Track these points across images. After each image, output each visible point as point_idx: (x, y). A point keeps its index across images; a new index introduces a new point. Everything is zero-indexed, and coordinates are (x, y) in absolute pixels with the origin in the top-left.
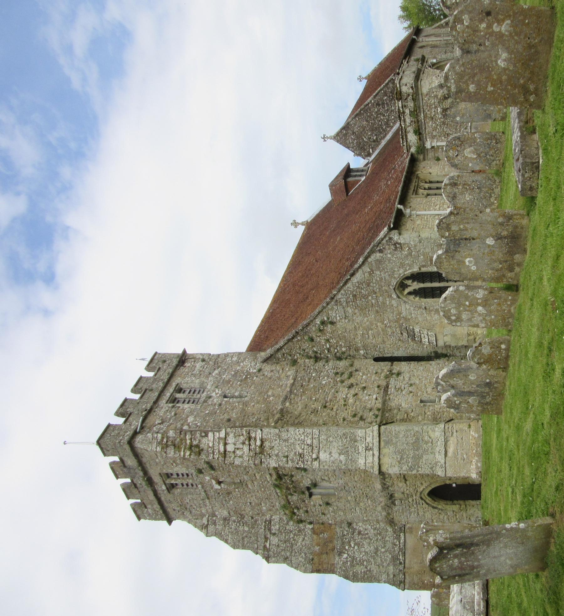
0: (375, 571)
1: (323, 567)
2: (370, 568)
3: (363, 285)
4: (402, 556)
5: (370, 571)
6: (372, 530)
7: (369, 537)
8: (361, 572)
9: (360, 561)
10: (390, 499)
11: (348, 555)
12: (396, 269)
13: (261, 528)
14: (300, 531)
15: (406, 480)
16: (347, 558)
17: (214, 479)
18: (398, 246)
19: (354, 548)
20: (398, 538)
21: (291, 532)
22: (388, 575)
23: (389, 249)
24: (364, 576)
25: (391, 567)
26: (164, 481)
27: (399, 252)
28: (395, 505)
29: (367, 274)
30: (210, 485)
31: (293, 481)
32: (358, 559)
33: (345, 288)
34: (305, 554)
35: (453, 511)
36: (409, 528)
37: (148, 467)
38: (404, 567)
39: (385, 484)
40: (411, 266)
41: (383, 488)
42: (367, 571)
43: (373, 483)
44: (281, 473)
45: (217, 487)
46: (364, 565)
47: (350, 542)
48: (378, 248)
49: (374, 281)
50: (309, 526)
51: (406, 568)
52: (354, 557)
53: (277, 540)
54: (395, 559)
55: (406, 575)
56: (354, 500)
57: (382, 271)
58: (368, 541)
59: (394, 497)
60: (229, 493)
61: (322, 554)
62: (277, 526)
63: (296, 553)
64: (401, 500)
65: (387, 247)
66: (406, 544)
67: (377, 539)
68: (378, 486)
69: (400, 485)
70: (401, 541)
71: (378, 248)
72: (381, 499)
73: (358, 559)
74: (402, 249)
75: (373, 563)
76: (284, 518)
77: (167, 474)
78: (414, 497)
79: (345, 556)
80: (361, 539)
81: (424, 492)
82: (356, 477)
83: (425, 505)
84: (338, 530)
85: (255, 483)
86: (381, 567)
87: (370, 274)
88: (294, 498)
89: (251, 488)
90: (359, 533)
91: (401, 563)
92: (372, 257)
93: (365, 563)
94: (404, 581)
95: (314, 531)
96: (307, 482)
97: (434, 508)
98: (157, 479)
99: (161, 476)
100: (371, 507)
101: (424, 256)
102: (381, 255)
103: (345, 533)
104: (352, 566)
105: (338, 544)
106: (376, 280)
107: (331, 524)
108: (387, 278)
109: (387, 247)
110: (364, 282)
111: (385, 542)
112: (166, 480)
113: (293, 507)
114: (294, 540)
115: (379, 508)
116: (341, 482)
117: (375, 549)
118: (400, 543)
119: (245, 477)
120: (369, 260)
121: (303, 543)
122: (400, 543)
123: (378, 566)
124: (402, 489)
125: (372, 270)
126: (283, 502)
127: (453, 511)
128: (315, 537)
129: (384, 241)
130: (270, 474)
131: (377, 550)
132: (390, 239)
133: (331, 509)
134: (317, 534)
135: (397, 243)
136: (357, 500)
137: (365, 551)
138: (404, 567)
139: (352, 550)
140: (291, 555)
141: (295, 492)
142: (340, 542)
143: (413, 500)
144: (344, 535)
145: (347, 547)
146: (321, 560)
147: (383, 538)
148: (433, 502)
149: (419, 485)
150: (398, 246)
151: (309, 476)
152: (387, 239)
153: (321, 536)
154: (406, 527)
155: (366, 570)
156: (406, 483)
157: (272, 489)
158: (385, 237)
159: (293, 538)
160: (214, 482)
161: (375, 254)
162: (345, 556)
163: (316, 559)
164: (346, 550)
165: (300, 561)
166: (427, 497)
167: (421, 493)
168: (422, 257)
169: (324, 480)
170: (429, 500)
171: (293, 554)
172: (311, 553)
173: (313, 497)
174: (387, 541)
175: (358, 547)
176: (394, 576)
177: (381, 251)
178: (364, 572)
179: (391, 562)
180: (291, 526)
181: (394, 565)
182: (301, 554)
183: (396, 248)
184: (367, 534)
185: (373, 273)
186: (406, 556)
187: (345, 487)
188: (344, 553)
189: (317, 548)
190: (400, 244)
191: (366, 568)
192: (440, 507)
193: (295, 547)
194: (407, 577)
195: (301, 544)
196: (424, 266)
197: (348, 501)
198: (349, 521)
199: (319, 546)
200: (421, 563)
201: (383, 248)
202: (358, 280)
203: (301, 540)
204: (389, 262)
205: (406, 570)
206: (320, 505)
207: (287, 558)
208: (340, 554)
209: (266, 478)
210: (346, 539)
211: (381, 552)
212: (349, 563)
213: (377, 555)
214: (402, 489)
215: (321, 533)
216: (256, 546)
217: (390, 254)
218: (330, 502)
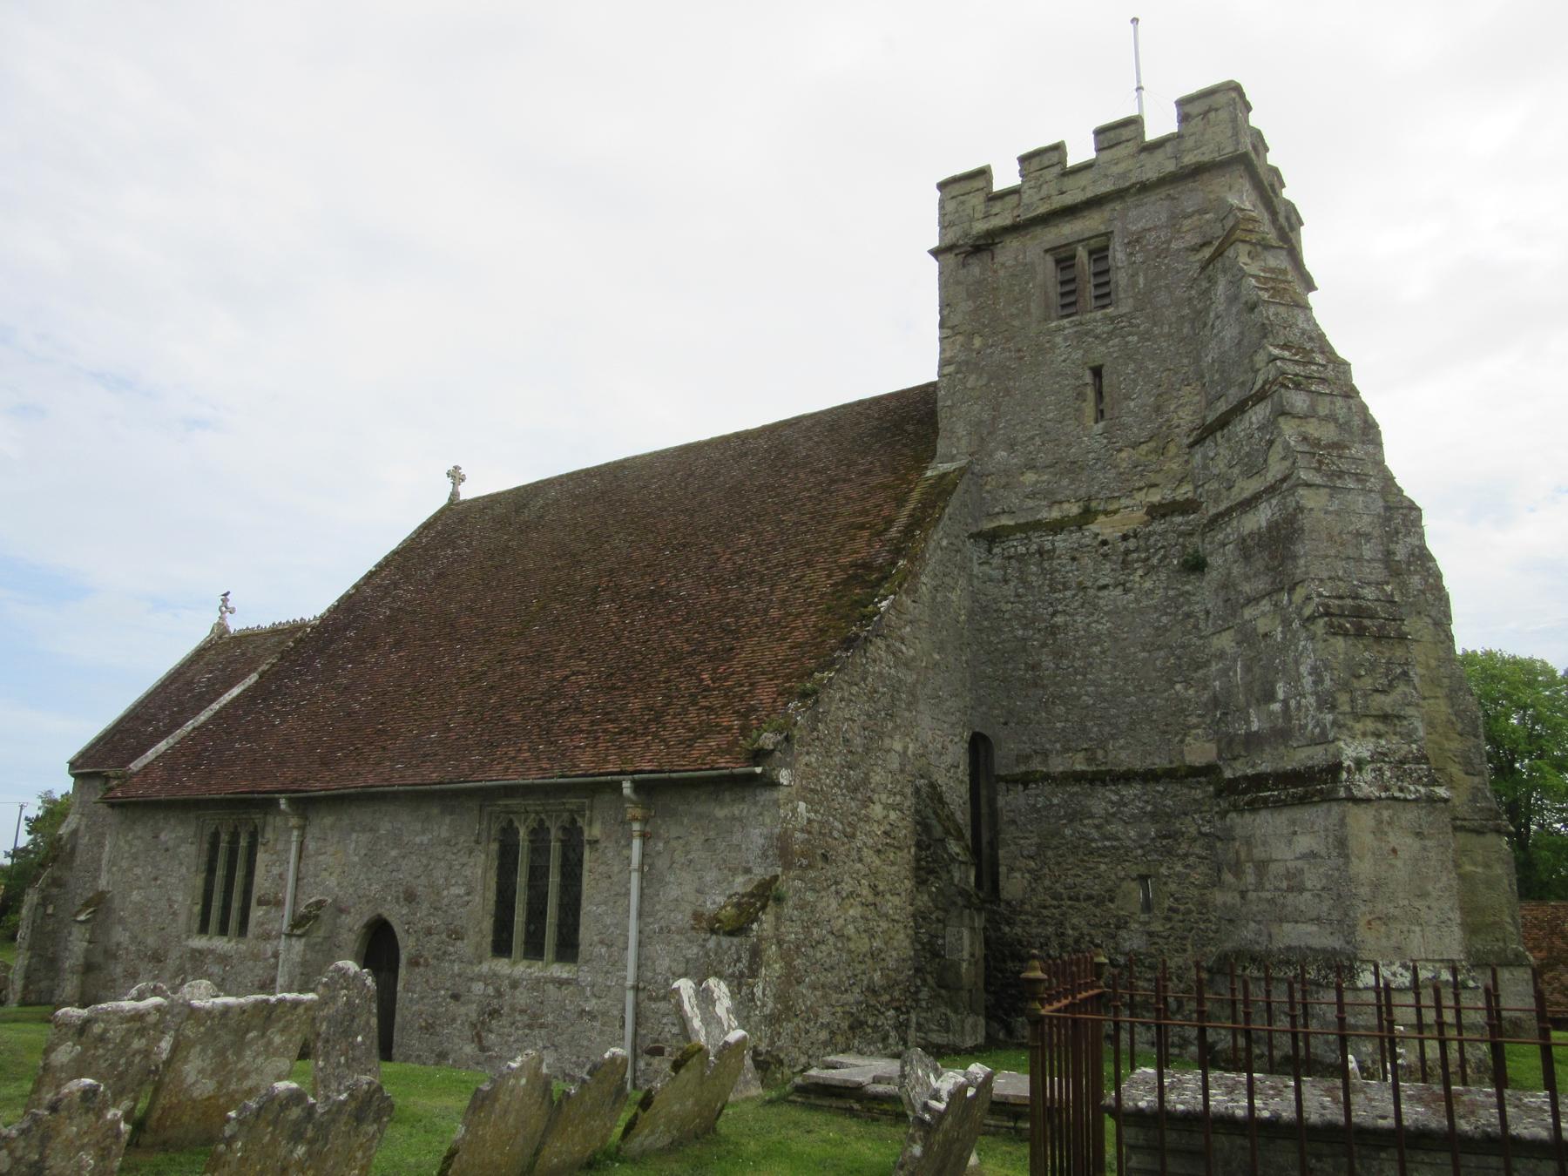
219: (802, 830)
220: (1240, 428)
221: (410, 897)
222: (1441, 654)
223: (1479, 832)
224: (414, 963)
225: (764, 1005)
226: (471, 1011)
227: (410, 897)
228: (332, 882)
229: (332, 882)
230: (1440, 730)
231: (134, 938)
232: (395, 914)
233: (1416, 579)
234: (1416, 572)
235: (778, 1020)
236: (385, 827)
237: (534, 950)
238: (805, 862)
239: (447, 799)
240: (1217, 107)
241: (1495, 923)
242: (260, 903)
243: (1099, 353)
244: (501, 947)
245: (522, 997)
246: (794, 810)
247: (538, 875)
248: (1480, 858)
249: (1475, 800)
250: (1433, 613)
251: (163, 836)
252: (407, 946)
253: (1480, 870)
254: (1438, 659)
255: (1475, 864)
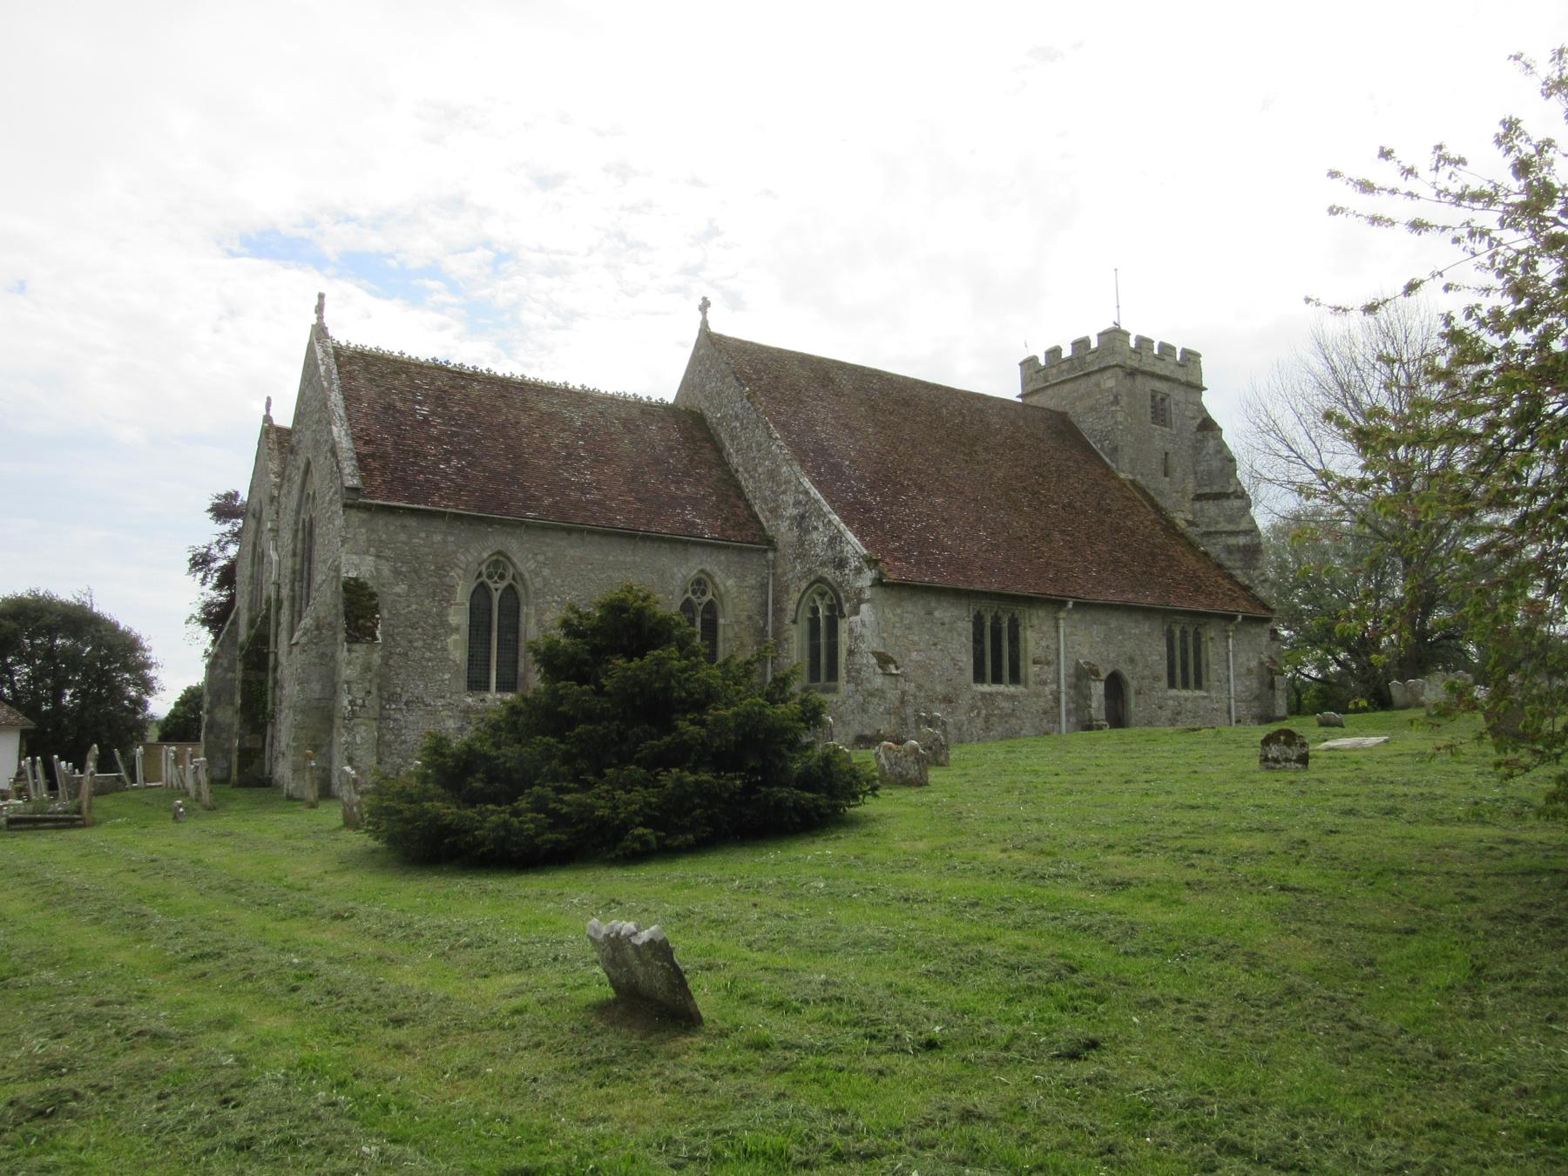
220: (1226, 503)
221: (1132, 660)
224: (1138, 693)
226: (1167, 713)
227: (1132, 660)
228: (1085, 651)
229: (1085, 651)
231: (919, 687)
232: (1126, 670)
236: (1114, 624)
237: (1186, 686)
239: (1148, 612)
240: (1191, 358)
242: (1035, 662)
243: (1169, 447)
244: (1172, 685)
245: (1189, 705)
247: (1184, 652)
251: (937, 614)
252: (1133, 685)
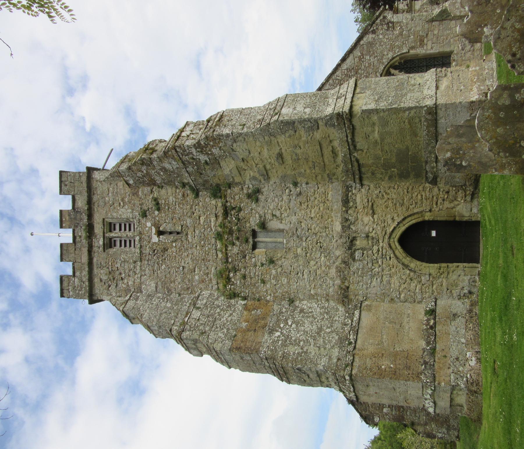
0: (313, 354)
1: (245, 345)
2: (307, 350)
3: (351, 72)
4: (354, 335)
5: (306, 352)
6: (318, 309)
7: (313, 316)
8: (294, 353)
9: (295, 341)
10: (350, 248)
11: (282, 333)
12: (386, 53)
13: (186, 305)
14: (229, 306)
15: (374, 213)
16: (279, 336)
17: (154, 226)
18: (390, 25)
19: (291, 326)
20: (351, 317)
21: (219, 306)
22: (330, 358)
23: (382, 29)
24: (297, 358)
25: (337, 350)
26: (104, 233)
27: (391, 32)
28: (354, 260)
29: (357, 60)
30: (149, 237)
31: (239, 220)
32: (293, 339)
33: (333, 77)
34: (228, 329)
35: (430, 275)
36: (367, 306)
37: (96, 210)
38: (355, 348)
39: (347, 220)
40: (399, 47)
41: (343, 227)
42: (302, 352)
43: (332, 221)
44: (228, 204)
45: (155, 239)
46: (299, 346)
47: (287, 320)
48: (372, 29)
49: (363, 67)
50: (241, 302)
51: (357, 350)
52: (288, 336)
53: (199, 313)
54: (343, 341)
55: (356, 357)
56: (304, 254)
57: (372, 55)
58: (310, 319)
59: (355, 244)
60: (165, 250)
61: (249, 330)
62: (205, 301)
63: (217, 328)
64: (363, 249)
65: (380, 27)
66: (361, 322)
67: (323, 318)
68: (338, 227)
69: (366, 219)
70: (355, 319)
71: (372, 29)
72: (338, 253)
73: (293, 339)
74: (394, 28)
75: (312, 344)
76: (216, 294)
77: (110, 224)
78: (381, 244)
79: (278, 334)
80: (303, 317)
81: (394, 235)
82: (313, 211)
83: (394, 261)
84: (276, 307)
85: (197, 232)
86: (322, 349)
87: (360, 59)
88: (235, 250)
89: (190, 240)
90: (302, 311)
91: (350, 343)
92: (365, 39)
93: (302, 343)
94: (352, 363)
95: (246, 308)
96: (253, 222)
97: (406, 266)
98: (98, 229)
99: (104, 225)
100: (323, 268)
101: (414, 36)
102: (374, 36)
103: (284, 310)
104: (284, 345)
105: (271, 322)
106: (365, 66)
107: (268, 301)
108: (376, 62)
109: (380, 27)
110: (353, 68)
111: (332, 323)
112: (107, 233)
113: (230, 267)
114: (219, 315)
115: (333, 271)
116: (294, 219)
117: (318, 328)
118: (352, 321)
119: (189, 221)
120: (362, 42)
121: (229, 319)
122: (352, 321)
123: (319, 348)
124: (367, 228)
125: (362, 54)
126: (220, 266)
127: (430, 275)
128: (245, 313)
129: (378, 21)
130: (216, 216)
131: (320, 329)
132: (385, 17)
133: (274, 272)
134: (249, 310)
135: (390, 22)
136: (308, 255)
137: (304, 331)
138: (355, 348)
139: (287, 329)
140: (210, 330)
141: (238, 239)
142: (275, 319)
143: (378, 250)
144: (282, 313)
145: (282, 325)
146: (246, 337)
147: (330, 318)
148: (404, 255)
149: (390, 221)
150: (390, 25)
151: (259, 209)
152: (381, 17)
153: (253, 312)
154: (363, 305)
155: (301, 351)
156: (373, 217)
157: (213, 240)
158: (380, 15)
159: (218, 313)
160: (154, 230)
161: (367, 36)
162: (278, 334)
163: (239, 336)
164: (280, 328)
165: (220, 337)
166: (397, 244)
167: (390, 238)
168: (412, 37)
169: (275, 216)
170: (399, 251)
171: (213, 329)
172: (235, 330)
173: (257, 250)
174: (336, 320)
175: (297, 325)
176: (339, 359)
177: (374, 32)
178: (298, 353)
179: (337, 344)
180: (222, 301)
181: (340, 348)
182: (222, 329)
183: (388, 27)
184: (312, 312)
185: (363, 58)
186: (359, 335)
187: (297, 230)
188: (277, 331)
189: (244, 324)
190: (393, 23)
191: (302, 349)
192: (412, 265)
193: (218, 322)
194: (357, 359)
195: (226, 319)
196: (413, 48)
197: (296, 256)
198: (292, 296)
199: (248, 322)
200: (379, 344)
201: (377, 29)
202: (348, 66)
203: (227, 315)
204: (380, 45)
205: (356, 351)
206: (262, 265)
207: (205, 332)
208: (271, 332)
209: (210, 221)
210: (283, 316)
211: (325, 332)
212: (280, 342)
213: (320, 336)
214: (367, 228)
215: (254, 309)
216: (173, 322)
217: (382, 34)
218: (275, 259)
219: (392, 410)
222: (251, 139)
223: (353, 129)
225: (444, 433)
230: (296, 142)
233: (214, 150)
234: (210, 150)
235: (449, 426)
238: (402, 409)
241: (409, 123)
246: (386, 414)
248: (370, 129)
249: (334, 125)
250: (230, 143)
253: (377, 129)
254: (256, 141)
255: (373, 131)
